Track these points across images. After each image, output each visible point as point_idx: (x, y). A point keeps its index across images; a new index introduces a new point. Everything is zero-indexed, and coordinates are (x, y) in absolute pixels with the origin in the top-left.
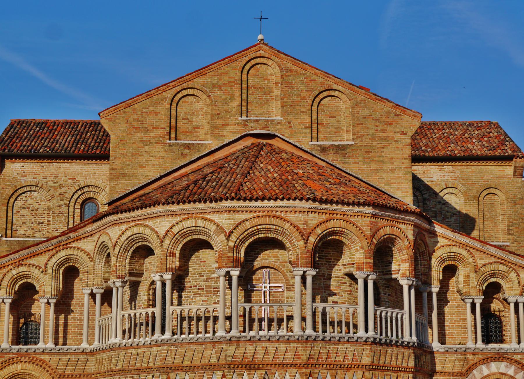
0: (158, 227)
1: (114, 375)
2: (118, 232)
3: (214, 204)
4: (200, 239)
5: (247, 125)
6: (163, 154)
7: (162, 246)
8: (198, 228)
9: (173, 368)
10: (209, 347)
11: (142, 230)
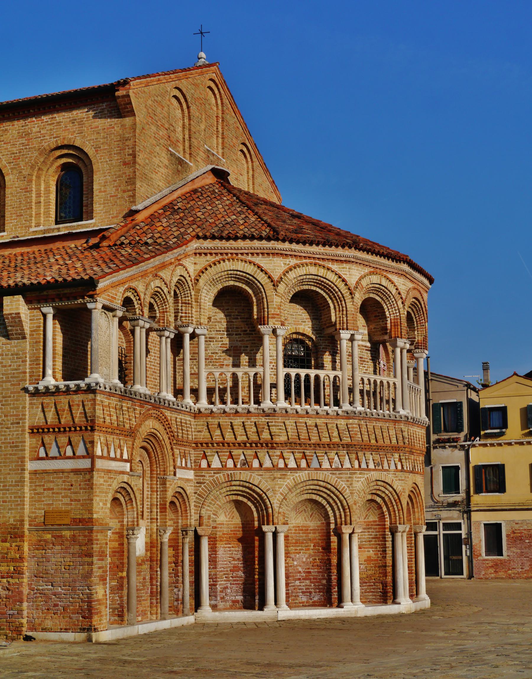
0: (346, 274)
1: (273, 448)
2: (283, 265)
3: (394, 264)
4: (375, 299)
5: (208, 156)
6: (166, 162)
7: (352, 298)
8: (381, 287)
9: (363, 447)
10: (391, 425)
11: (322, 272)
